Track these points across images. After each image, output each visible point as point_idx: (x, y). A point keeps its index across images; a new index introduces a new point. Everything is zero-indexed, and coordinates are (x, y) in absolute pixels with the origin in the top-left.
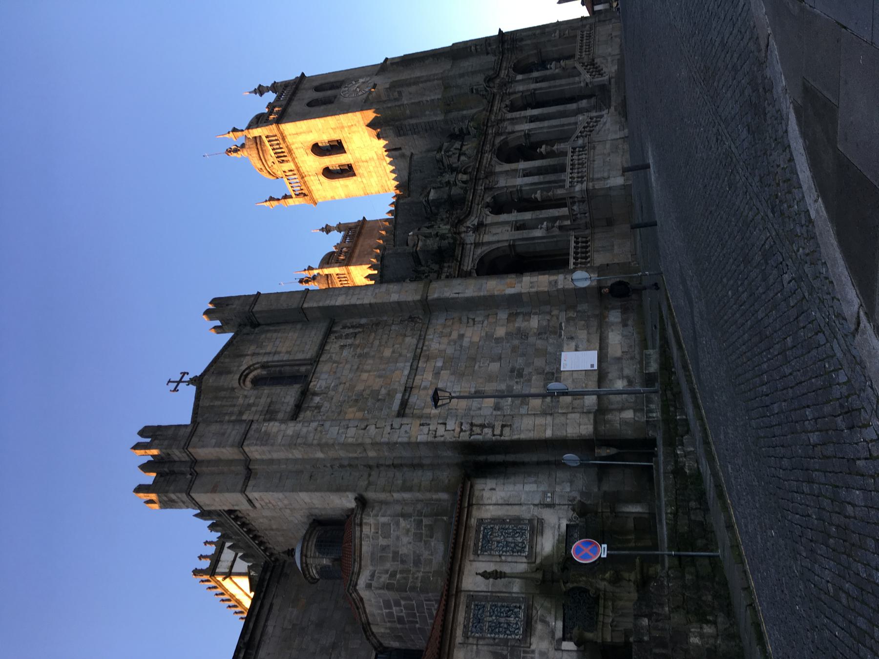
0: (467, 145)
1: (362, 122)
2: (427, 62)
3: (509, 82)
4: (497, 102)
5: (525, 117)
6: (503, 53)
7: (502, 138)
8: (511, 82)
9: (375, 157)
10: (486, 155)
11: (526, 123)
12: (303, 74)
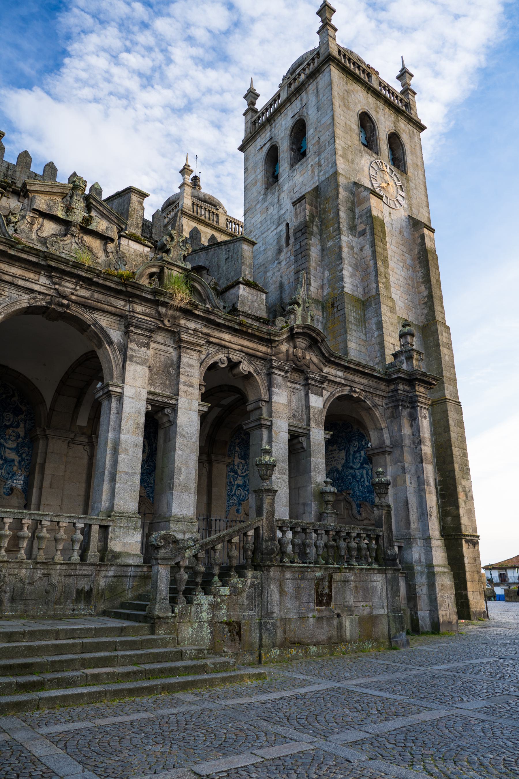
0: (105, 250)
1: (323, 178)
2: (423, 287)
3: (307, 379)
4: (246, 343)
5: (178, 395)
6: (389, 381)
7: (116, 335)
8: (306, 385)
9: (282, 212)
10: (43, 280)
11: (149, 393)
12: (422, 128)
